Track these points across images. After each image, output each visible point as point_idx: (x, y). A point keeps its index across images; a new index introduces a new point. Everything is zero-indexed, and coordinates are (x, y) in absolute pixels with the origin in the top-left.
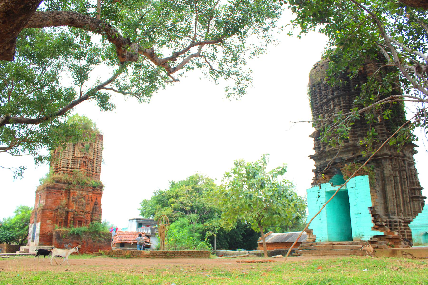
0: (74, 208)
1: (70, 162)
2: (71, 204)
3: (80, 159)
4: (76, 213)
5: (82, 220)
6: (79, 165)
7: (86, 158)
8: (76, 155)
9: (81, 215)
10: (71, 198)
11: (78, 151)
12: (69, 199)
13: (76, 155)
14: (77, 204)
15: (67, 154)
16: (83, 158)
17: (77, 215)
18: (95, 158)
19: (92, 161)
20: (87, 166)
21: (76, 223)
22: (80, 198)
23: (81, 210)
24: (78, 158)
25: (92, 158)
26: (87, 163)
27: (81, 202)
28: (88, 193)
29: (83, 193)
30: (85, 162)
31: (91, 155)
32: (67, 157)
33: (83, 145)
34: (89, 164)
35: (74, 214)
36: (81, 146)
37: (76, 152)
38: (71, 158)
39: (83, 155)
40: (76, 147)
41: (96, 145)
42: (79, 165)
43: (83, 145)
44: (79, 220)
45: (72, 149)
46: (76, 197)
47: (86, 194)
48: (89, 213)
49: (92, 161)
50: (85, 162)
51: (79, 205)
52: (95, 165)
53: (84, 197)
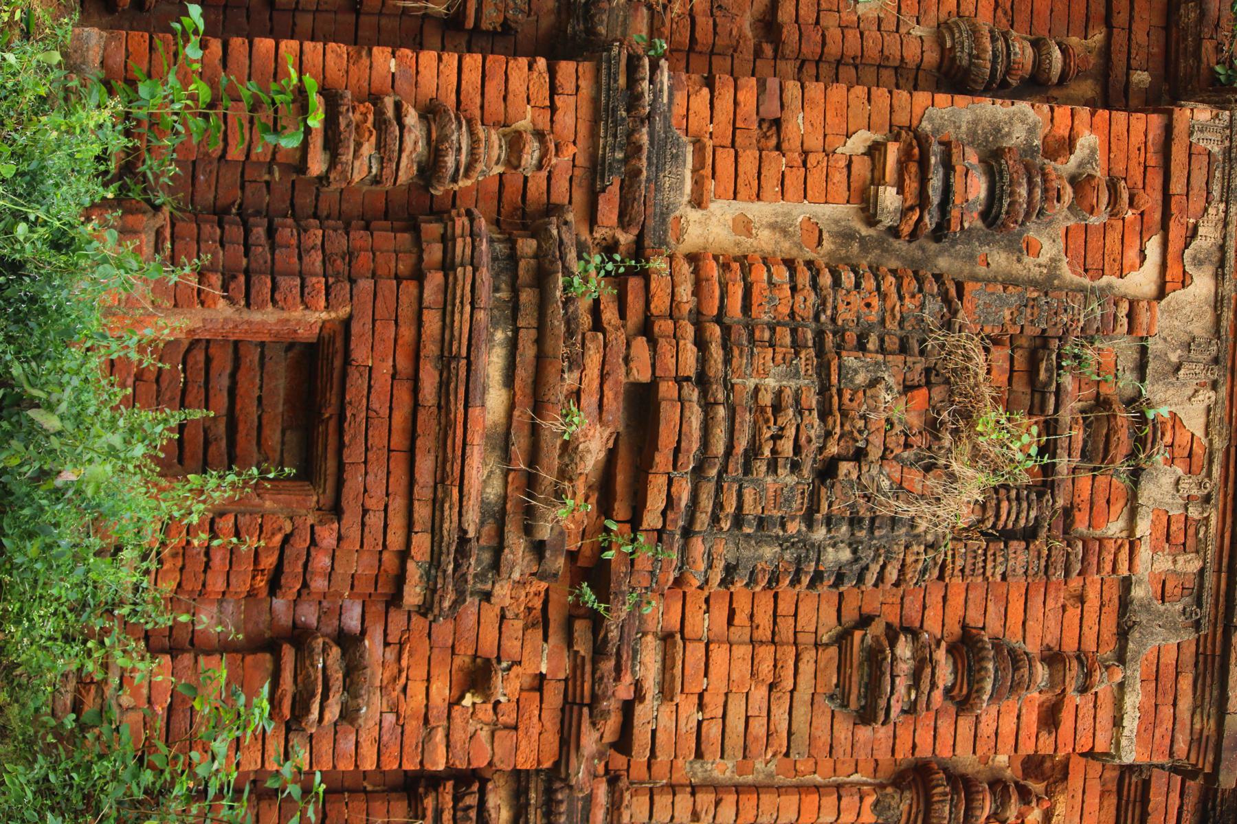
0: (709, 226)
2: (841, 124)
4: (587, 280)
5: (369, 482)
9: (514, 416)
10: (1022, 120)
12: (954, 78)
14: (853, 306)
17: (531, 283)
21: (241, 282)
22: (1034, 369)
23: (680, 420)
27: (946, 418)
28: (1164, 640)
29: (1163, 487)
35: (524, 217)
44: (375, 357)
46: (1048, 246)
47: (1152, 564)
48: (577, 706)
51: (824, 344)
53: (1029, 520)
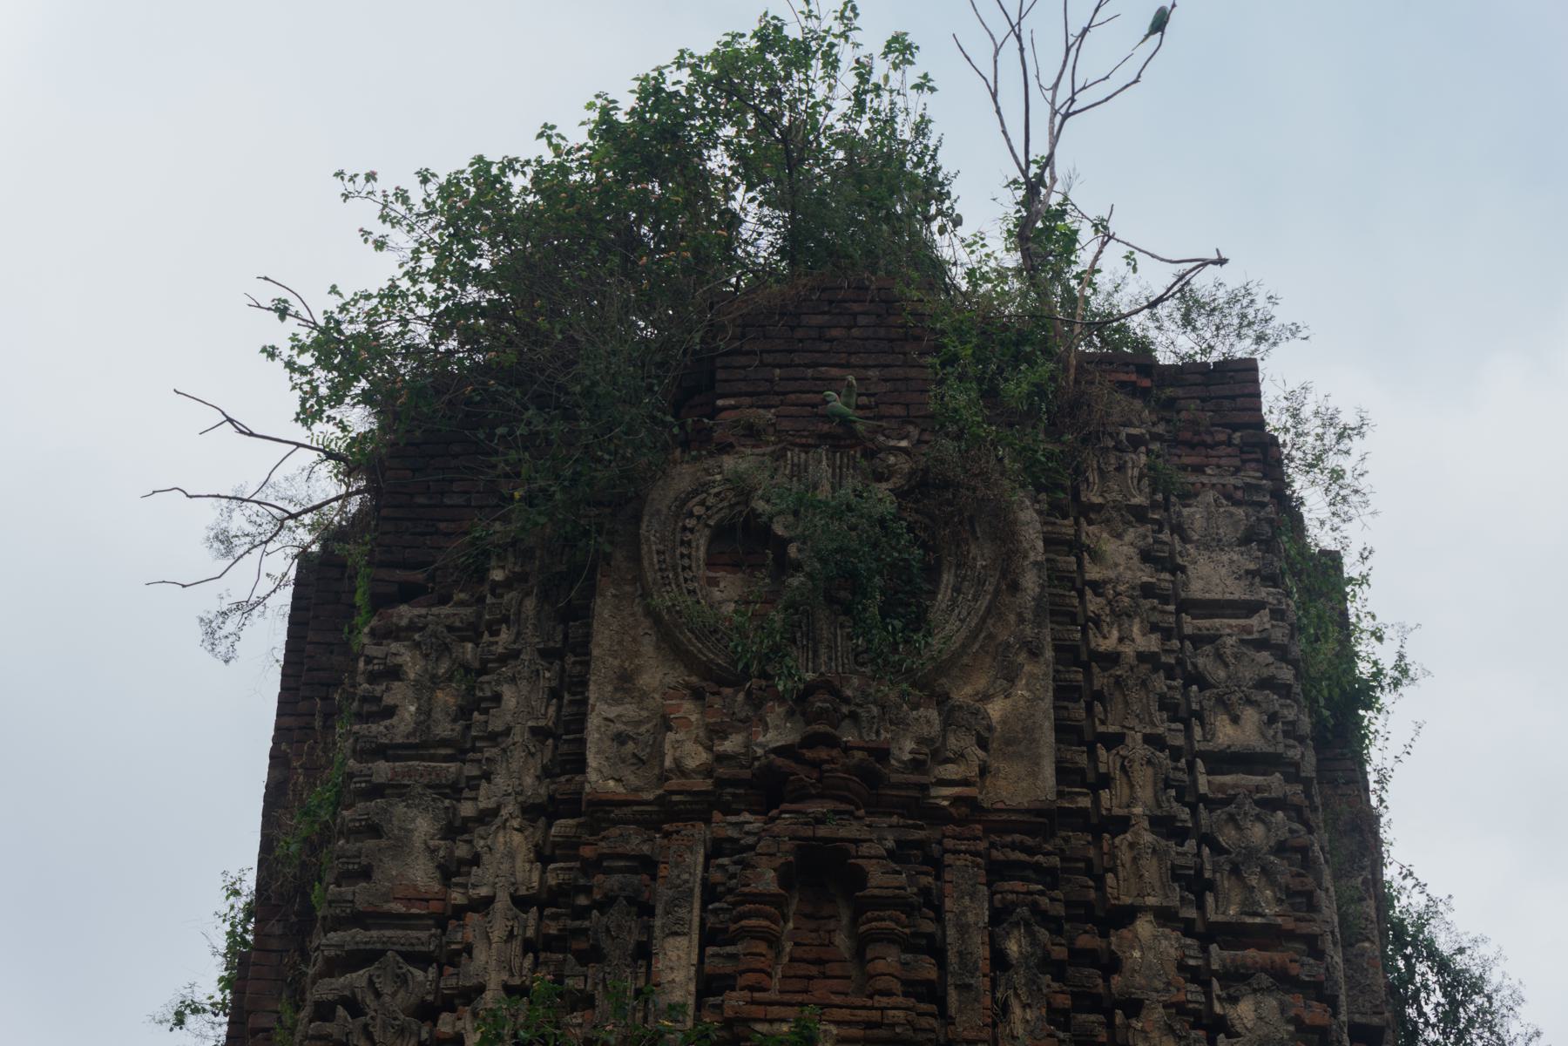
1: (491, 959)
3: (700, 830)
6: (677, 962)
7: (870, 785)
8: (600, 777)
11: (656, 675)
13: (600, 777)
15: (423, 826)
16: (767, 787)
18: (1137, 794)
19: (1055, 863)
20: (888, 960)
24: (666, 814)
25: (1025, 783)
26: (879, 879)
30: (822, 872)
31: (1001, 734)
32: (421, 874)
33: (744, 539)
34: (968, 907)
36: (726, 593)
37: (603, 713)
38: (509, 859)
39: (777, 732)
40: (609, 623)
41: (1118, 556)
42: (677, 962)
43: (744, 539)
45: (518, 702)
49: (1055, 863)
50: (822, 872)
52: (1149, 948)
